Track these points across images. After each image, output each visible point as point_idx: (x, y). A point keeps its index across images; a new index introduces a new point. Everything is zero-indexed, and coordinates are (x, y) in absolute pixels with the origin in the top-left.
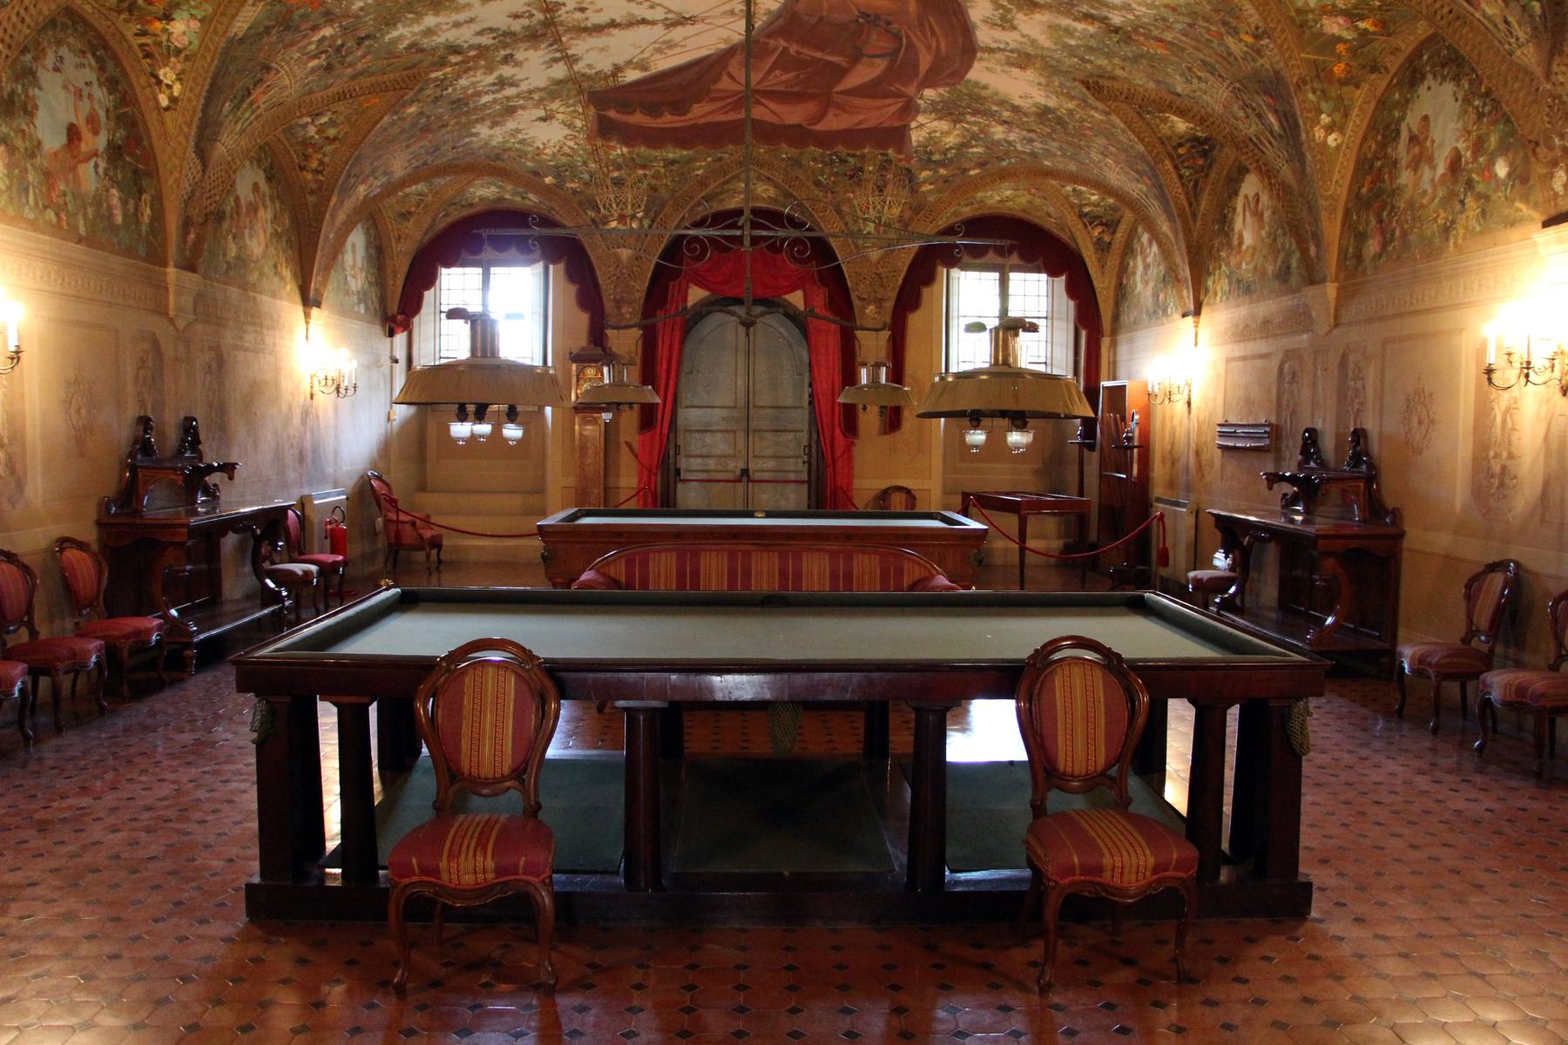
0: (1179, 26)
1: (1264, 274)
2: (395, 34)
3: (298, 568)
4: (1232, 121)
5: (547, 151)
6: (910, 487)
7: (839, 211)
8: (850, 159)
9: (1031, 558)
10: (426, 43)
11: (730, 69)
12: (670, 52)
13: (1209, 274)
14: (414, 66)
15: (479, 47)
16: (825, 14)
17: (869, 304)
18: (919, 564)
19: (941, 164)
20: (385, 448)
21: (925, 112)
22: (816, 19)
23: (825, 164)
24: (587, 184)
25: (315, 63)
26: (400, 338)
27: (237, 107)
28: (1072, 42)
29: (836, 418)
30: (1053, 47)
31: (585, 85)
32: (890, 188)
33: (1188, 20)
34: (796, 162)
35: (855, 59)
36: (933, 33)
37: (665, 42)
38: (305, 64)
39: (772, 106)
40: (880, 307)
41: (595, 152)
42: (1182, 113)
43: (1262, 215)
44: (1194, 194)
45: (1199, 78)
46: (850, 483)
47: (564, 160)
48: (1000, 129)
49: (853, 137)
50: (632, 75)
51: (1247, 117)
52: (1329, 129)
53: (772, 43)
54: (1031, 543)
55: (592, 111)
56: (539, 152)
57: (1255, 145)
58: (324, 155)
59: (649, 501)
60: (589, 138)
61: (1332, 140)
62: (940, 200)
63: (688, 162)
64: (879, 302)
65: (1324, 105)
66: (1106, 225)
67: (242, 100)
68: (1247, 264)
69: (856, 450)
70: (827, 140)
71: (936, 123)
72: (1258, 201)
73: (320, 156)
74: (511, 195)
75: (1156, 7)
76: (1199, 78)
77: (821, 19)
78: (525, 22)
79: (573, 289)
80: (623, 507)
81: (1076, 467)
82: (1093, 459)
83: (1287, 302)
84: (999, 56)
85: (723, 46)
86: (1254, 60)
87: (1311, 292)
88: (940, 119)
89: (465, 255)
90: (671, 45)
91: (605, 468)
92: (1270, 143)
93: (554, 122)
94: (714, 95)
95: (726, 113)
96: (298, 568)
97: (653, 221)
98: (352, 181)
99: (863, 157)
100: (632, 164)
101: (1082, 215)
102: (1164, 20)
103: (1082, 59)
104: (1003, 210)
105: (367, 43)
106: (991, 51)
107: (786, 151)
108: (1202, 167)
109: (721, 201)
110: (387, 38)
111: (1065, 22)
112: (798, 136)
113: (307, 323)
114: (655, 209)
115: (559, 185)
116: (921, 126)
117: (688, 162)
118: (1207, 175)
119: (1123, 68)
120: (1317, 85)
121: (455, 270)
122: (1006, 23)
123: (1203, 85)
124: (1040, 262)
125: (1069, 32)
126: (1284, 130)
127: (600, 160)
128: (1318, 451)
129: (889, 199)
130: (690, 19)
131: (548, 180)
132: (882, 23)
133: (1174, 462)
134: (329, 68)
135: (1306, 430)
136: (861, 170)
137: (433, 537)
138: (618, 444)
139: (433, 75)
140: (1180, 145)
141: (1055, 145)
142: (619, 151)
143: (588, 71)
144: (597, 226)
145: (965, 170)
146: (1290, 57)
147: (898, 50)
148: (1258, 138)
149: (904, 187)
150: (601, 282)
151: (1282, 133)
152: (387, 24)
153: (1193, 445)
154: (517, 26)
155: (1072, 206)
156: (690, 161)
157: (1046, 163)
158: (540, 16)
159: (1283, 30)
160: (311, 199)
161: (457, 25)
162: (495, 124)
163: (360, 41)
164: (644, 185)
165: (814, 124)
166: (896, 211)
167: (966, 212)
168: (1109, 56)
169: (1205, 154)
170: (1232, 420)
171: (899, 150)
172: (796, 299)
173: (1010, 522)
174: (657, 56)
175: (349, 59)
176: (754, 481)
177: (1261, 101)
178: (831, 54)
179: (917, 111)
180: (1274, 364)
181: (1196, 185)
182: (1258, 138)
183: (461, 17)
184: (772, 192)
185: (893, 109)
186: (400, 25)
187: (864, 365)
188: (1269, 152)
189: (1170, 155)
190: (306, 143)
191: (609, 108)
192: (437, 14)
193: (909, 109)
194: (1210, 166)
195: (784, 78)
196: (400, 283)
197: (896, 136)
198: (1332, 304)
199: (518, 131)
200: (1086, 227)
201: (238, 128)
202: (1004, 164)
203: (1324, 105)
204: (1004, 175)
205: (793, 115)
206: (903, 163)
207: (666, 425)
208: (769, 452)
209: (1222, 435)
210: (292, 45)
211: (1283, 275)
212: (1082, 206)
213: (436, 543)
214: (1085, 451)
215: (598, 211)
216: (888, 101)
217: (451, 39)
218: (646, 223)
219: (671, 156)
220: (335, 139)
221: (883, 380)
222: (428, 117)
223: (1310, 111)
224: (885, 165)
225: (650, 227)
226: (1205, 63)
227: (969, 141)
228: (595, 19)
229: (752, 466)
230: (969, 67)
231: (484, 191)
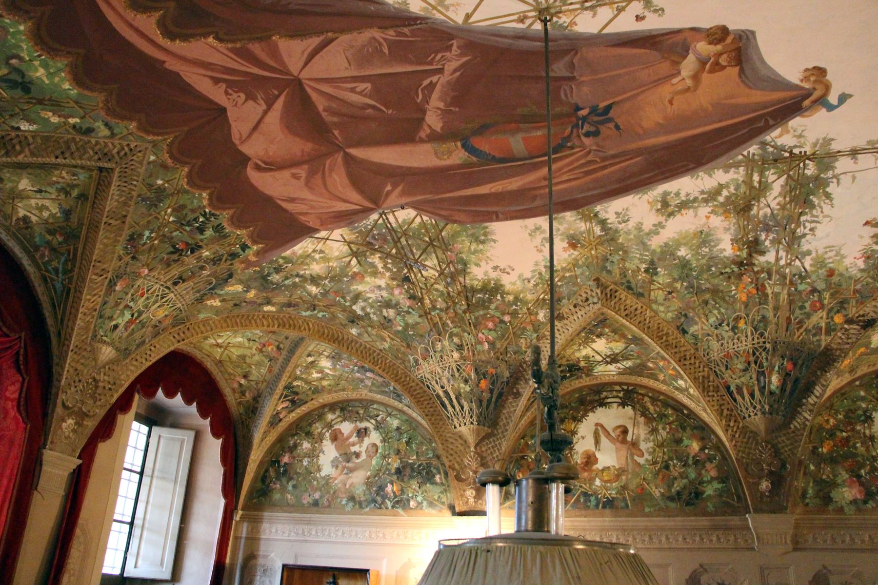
7: (112, 284)
11: (344, 38)
17: (69, 416)
36: (587, 173)
51: (745, 370)
64: (82, 416)
92: (752, 395)
94: (256, 48)
95: (216, 81)
151: (777, 392)
184: (37, 218)
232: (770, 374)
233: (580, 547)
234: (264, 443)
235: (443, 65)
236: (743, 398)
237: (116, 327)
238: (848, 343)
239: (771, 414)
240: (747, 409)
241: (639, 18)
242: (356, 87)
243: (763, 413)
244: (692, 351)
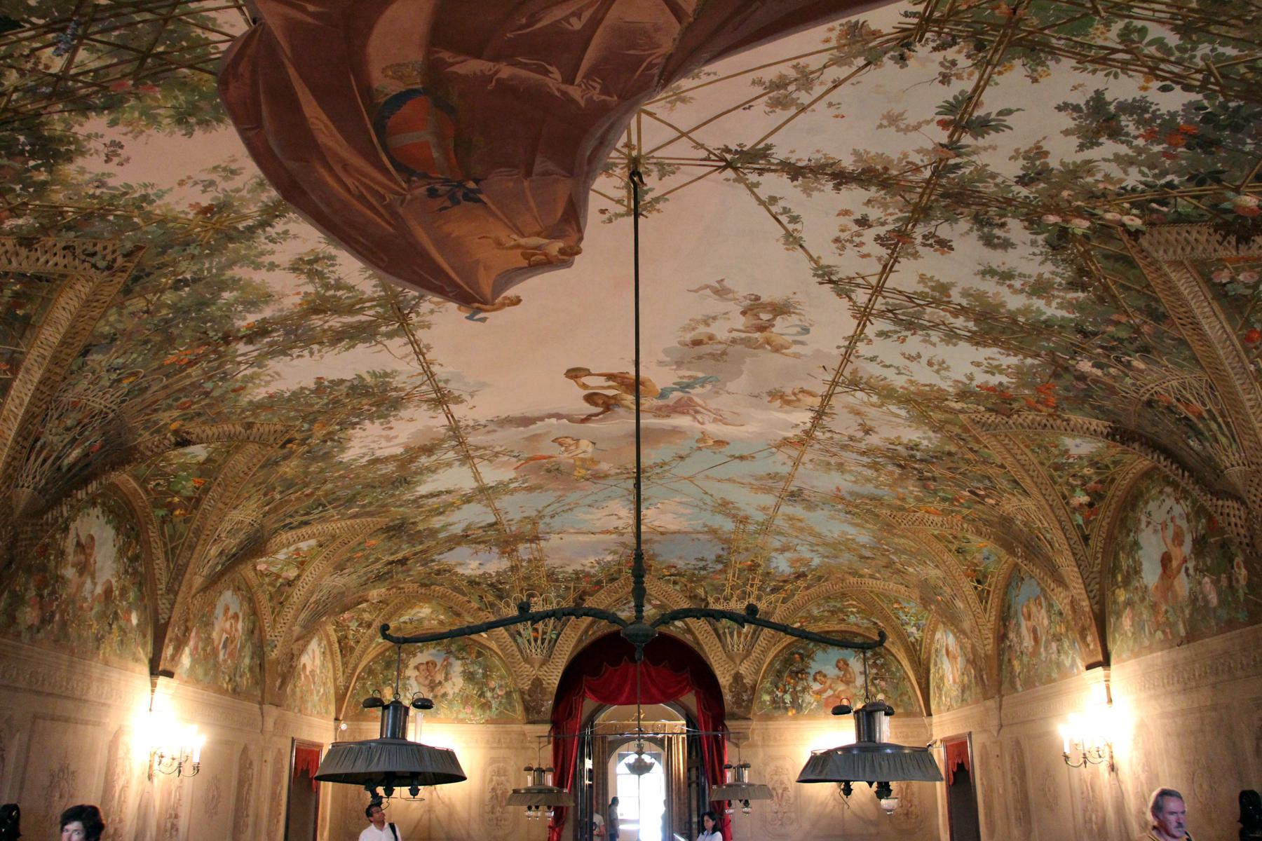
11: (676, 28)
12: (788, 70)
16: (526, 184)
27: (1199, 434)
36: (361, 198)
51: (68, 429)
57: (32, 448)
67: (1192, 427)
85: (685, 83)
92: (45, 461)
126: (69, 470)
130: (729, 165)
132: (441, 189)
148: (43, 448)
151: (64, 470)
174: (814, 63)
178: (485, 79)
182: (43, 448)
201: (1224, 440)
232: (78, 446)
233: (889, 751)
235: (579, 86)
236: (36, 461)
238: (152, 451)
239: (40, 493)
240: (27, 476)
241: (603, 212)
242: (580, 18)
243: (35, 489)
244: (59, 378)
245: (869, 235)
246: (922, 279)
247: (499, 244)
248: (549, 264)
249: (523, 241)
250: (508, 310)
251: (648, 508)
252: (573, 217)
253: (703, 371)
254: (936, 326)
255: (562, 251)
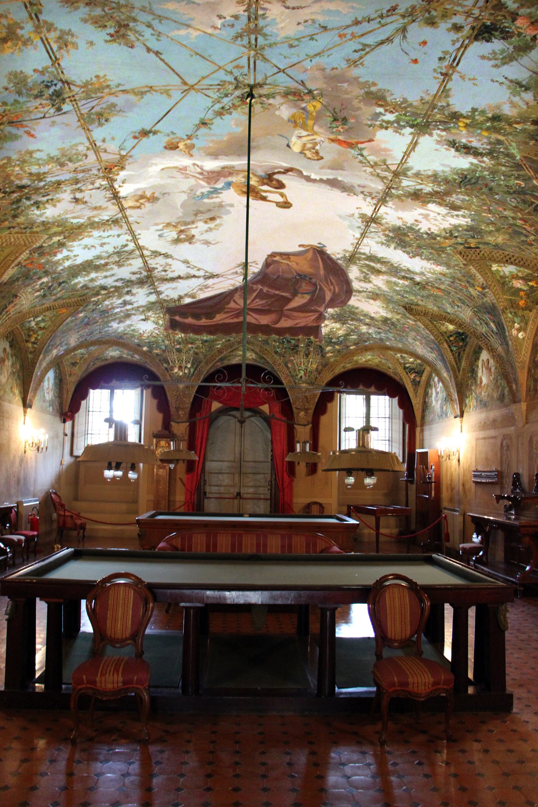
0: (447, 283)
1: (492, 398)
2: (76, 281)
3: (15, 538)
4: (474, 326)
5: (145, 335)
6: (321, 502)
7: (287, 367)
8: (293, 342)
9: (382, 539)
10: (91, 285)
11: (235, 298)
12: (206, 290)
13: (467, 397)
14: (84, 295)
15: (115, 287)
18: (325, 541)
19: (335, 343)
20: (59, 478)
21: (328, 319)
22: (275, 277)
23: (280, 343)
24: (164, 351)
25: (38, 293)
26: (69, 424)
28: (398, 289)
29: (285, 468)
30: (388, 290)
31: (165, 304)
32: (312, 354)
33: (451, 280)
34: (266, 342)
35: (295, 294)
36: (332, 284)
37: (204, 286)
38: (33, 294)
39: (254, 315)
40: (307, 413)
41: (167, 336)
42: (451, 322)
43: (490, 369)
44: (458, 359)
45: (458, 306)
46: (291, 500)
47: (153, 339)
48: (365, 327)
49: (294, 331)
50: (188, 301)
52: (519, 330)
53: (255, 287)
54: (382, 531)
55: (167, 316)
56: (141, 335)
58: (38, 335)
59: (191, 508)
60: (165, 329)
61: (521, 335)
62: (336, 361)
63: (213, 341)
64: (306, 410)
65: (516, 319)
66: (417, 373)
68: (485, 392)
69: (294, 484)
70: (280, 332)
71: (334, 324)
72: (488, 363)
73: (36, 336)
74: (127, 355)
75: (436, 274)
76: (458, 306)
77: (279, 276)
78: (138, 276)
79: (155, 402)
80: (178, 511)
81: (404, 492)
82: (413, 488)
83: (504, 411)
84: (364, 294)
85: (231, 288)
86: (482, 298)
87: (514, 407)
88: (336, 322)
89: (102, 384)
90: (207, 287)
91: (169, 490)
93: (149, 321)
94: (226, 310)
96: (15, 538)
97: (195, 369)
98: (50, 348)
99: (298, 340)
100: (186, 342)
101: (405, 368)
102: (440, 279)
103: (403, 296)
104: (367, 365)
105: (63, 285)
106: (360, 292)
107: (261, 337)
108: (462, 347)
109: (229, 360)
110: (72, 283)
111: (394, 279)
112: (266, 330)
113: (25, 416)
114: (196, 363)
115: (150, 351)
116: (326, 326)
117: (213, 341)
118: (464, 350)
119: (422, 301)
120: (512, 310)
121: (98, 391)
122: (366, 279)
123: (460, 309)
124: (385, 390)
125: (396, 284)
127: (171, 340)
128: (520, 484)
129: (311, 360)
131: (145, 349)
132: (307, 279)
133: (452, 489)
134: (44, 296)
135: (515, 474)
136: (297, 346)
137: (81, 524)
138: (175, 480)
139: (93, 299)
140: (451, 336)
141: (392, 335)
142: (180, 335)
143: (166, 298)
144: (168, 371)
145: (348, 346)
146: (499, 298)
147: (315, 291)
149: (318, 354)
150: (169, 399)
152: (73, 277)
153: (461, 481)
154: (134, 278)
155: (400, 364)
156: (214, 341)
157: (387, 343)
158: (145, 274)
159: (495, 286)
160: (30, 356)
161: (106, 277)
162: (120, 322)
163: (60, 284)
164: (192, 352)
165: (277, 323)
166: (314, 366)
167: (349, 366)
168: (415, 295)
169: (463, 340)
170: (480, 469)
171: (316, 336)
172: (265, 408)
173: (371, 520)
174: (200, 292)
175: (55, 292)
176: (243, 499)
177: (486, 317)
178: (282, 292)
179: (325, 319)
180: (499, 442)
181: (459, 355)
183: (108, 274)
185: (313, 318)
186: (79, 277)
187: (299, 442)
188: (492, 340)
189: (446, 340)
190: (30, 329)
191: (176, 315)
192: (97, 272)
193: (321, 318)
194: (466, 346)
195: (261, 303)
196: (70, 396)
197: (315, 330)
198: (524, 414)
199: (132, 325)
200: (407, 374)
202: (367, 343)
203: (516, 319)
204: (367, 349)
205: (264, 320)
206: (318, 343)
207: (200, 470)
208: (251, 484)
209: (475, 476)
210: (28, 285)
211: (502, 398)
212: (405, 364)
213: (83, 527)
214: (409, 484)
215: (169, 364)
216: (311, 314)
217: (103, 283)
218: (192, 370)
219: (205, 338)
220: (44, 328)
221: (308, 450)
222: (89, 318)
223: (509, 322)
224: (308, 345)
225: (194, 372)
226: (460, 299)
227: (350, 333)
228: (171, 275)
229: (242, 491)
230: (349, 299)
231: (113, 353)
234: (418, 394)
237: (301, 377)
245: (160, 269)
246: (130, 265)
247: (297, 264)
248: (281, 254)
249: (288, 262)
250: (306, 244)
251: (236, 17)
252: (267, 264)
253: (205, 203)
254: (109, 257)
255: (275, 257)
